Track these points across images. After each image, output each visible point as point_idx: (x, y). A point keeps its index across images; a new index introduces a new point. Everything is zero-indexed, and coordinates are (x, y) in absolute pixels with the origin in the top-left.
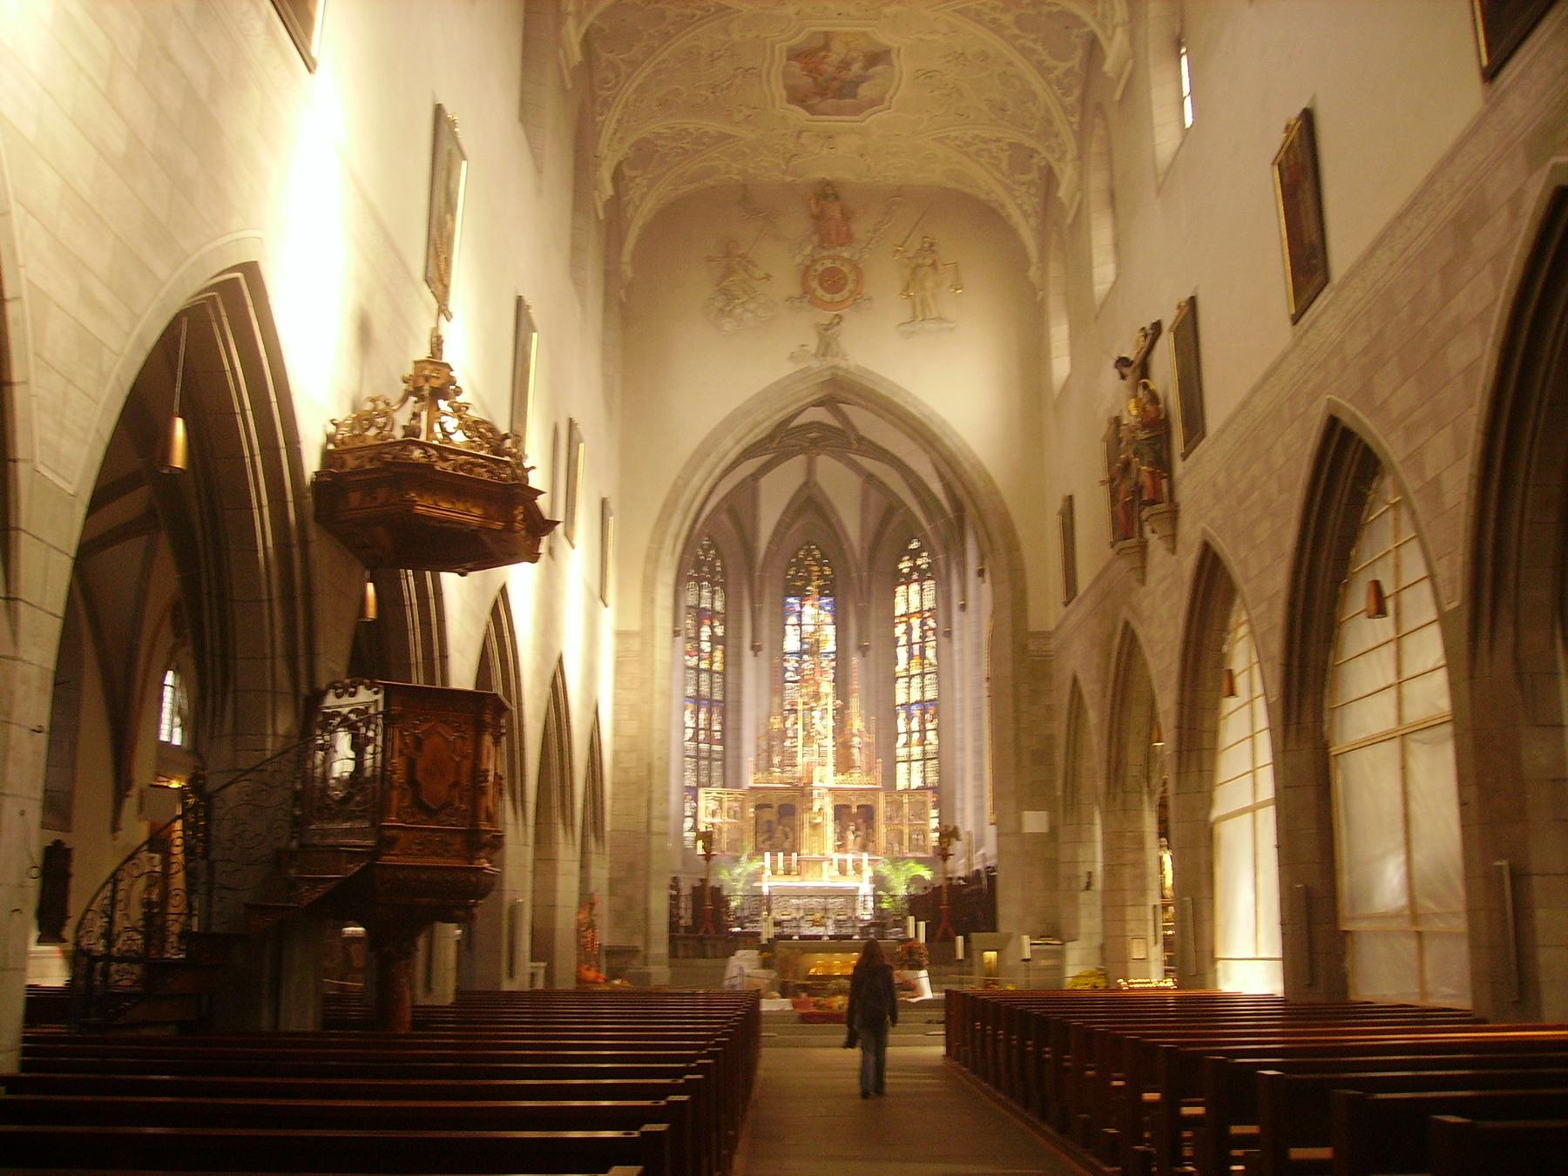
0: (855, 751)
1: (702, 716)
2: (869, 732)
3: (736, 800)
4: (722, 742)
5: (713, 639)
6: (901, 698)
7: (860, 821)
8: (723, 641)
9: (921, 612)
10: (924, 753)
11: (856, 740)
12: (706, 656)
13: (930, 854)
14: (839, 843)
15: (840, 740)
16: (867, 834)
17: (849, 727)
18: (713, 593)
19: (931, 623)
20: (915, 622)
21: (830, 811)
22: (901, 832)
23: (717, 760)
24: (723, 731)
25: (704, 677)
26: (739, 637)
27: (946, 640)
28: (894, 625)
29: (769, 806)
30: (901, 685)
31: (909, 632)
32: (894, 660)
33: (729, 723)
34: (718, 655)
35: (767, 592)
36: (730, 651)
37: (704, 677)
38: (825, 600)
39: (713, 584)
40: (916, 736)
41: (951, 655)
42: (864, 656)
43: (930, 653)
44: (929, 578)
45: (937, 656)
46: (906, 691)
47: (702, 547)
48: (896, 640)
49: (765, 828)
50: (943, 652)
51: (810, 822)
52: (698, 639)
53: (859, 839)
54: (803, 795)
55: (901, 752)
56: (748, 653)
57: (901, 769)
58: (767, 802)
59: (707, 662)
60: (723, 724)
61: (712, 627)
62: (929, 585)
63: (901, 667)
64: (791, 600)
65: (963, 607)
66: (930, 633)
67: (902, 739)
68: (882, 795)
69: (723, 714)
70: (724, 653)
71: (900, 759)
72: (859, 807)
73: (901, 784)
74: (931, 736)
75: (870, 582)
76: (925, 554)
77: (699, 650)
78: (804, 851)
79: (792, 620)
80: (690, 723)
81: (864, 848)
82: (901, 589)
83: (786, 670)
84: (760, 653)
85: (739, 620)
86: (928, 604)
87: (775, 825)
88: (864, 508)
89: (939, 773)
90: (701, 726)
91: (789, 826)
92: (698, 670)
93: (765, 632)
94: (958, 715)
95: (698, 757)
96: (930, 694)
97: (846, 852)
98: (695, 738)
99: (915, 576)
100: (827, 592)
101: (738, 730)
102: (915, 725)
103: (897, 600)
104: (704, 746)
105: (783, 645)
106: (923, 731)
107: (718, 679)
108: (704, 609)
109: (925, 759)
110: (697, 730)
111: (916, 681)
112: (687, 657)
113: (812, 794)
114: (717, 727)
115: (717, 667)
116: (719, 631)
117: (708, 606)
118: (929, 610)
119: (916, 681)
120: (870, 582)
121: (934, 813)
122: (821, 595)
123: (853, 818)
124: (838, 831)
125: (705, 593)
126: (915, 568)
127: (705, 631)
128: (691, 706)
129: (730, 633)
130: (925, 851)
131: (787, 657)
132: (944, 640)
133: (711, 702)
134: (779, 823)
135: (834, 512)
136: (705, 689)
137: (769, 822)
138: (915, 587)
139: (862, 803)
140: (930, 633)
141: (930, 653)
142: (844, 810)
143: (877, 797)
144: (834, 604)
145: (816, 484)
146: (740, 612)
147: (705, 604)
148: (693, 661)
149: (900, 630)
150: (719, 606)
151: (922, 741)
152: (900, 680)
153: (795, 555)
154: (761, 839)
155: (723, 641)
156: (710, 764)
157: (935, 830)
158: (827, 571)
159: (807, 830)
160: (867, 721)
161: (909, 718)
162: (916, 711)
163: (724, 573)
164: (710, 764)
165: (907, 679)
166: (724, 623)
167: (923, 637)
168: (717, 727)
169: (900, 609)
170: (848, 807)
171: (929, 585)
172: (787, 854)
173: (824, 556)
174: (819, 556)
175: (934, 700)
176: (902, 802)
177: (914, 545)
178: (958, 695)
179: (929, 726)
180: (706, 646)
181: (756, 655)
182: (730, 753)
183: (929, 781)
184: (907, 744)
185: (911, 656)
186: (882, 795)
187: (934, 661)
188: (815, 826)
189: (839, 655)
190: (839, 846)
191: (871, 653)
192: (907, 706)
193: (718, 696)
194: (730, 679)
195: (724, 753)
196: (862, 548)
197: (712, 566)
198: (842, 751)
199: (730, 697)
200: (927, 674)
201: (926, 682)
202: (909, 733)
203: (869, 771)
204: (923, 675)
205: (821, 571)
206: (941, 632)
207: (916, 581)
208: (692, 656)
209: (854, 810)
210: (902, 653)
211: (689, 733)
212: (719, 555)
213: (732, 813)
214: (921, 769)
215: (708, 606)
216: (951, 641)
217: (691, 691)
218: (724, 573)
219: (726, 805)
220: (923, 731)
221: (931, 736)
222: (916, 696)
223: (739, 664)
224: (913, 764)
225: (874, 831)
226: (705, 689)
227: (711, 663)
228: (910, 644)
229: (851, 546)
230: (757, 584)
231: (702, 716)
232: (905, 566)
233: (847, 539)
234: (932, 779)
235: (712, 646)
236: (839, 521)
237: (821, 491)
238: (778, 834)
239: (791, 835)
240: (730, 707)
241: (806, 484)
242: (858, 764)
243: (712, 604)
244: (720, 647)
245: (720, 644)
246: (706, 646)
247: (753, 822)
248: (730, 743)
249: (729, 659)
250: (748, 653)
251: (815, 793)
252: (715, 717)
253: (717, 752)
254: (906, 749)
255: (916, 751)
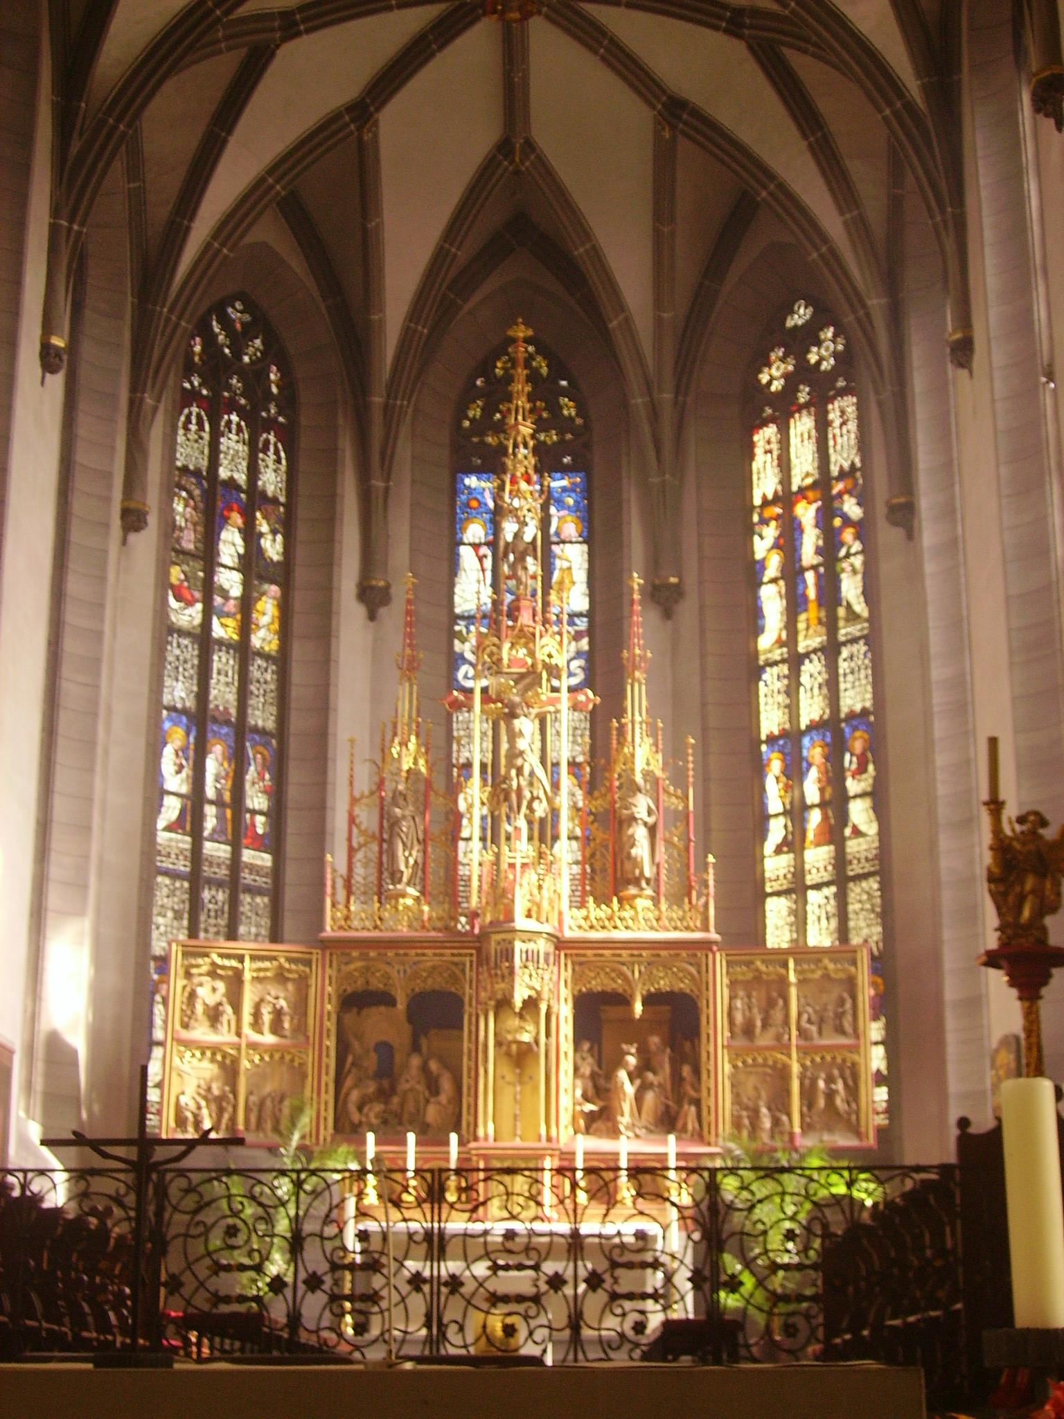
0: (640, 833)
1: (213, 765)
2: (679, 778)
3: (281, 977)
4: (275, 843)
5: (251, 563)
6: (771, 720)
7: (655, 1040)
8: (283, 574)
9: (823, 483)
10: (840, 861)
11: (641, 805)
12: (231, 606)
13: (871, 1141)
14: (589, 1107)
15: (599, 804)
16: (677, 1078)
17: (619, 768)
18: (255, 450)
19: (851, 508)
20: (806, 513)
21: (565, 1012)
22: (783, 1074)
23: (253, 891)
24: (276, 814)
25: (223, 662)
26: (327, 563)
27: (897, 534)
28: (749, 531)
29: (385, 999)
30: (771, 683)
31: (789, 541)
32: (755, 625)
33: (293, 793)
34: (267, 610)
35: (404, 450)
36: (300, 599)
37: (223, 662)
38: (559, 483)
39: (255, 425)
40: (815, 818)
41: (914, 574)
42: (668, 614)
43: (851, 588)
44: (842, 393)
45: (869, 593)
46: (782, 699)
47: (226, 323)
48: (762, 565)
49: (371, 1062)
50: (888, 568)
51: (498, 1044)
52: (208, 556)
53: (650, 1097)
54: (482, 958)
55: (776, 866)
56: (350, 611)
57: (777, 911)
58: (377, 984)
59: (231, 622)
60: (277, 794)
61: (250, 535)
62: (843, 409)
63: (767, 641)
64: (472, 481)
65: (963, 351)
66: (848, 535)
67: (777, 830)
68: (719, 962)
69: (279, 768)
70: (285, 609)
71: (776, 887)
72: (648, 1001)
73: (778, 933)
74: (860, 813)
75: (680, 426)
76: (829, 333)
77: (209, 589)
78: (487, 1128)
79: (475, 531)
80: (175, 781)
81: (667, 1122)
82: (766, 436)
83: (458, 659)
84: (383, 611)
85: (330, 521)
86: (843, 454)
87: (398, 1058)
88: (663, 209)
89: (886, 915)
90: (210, 793)
91: (442, 1060)
92: (204, 640)
93: (399, 553)
94: (940, 728)
95: (196, 879)
96: (855, 697)
97: (614, 1133)
98: (191, 820)
99: (803, 397)
100: (567, 460)
101: (319, 808)
102: (812, 790)
103: (756, 466)
104: (216, 850)
105: (452, 585)
106: (836, 803)
107: (263, 675)
108: (231, 483)
109: (841, 878)
110: (196, 800)
111: (812, 670)
112: (172, 602)
113: (508, 955)
114: (257, 800)
115: (264, 638)
116: (273, 548)
117: (241, 478)
118: (843, 475)
119: (812, 670)
120: (680, 426)
121: (876, 1030)
122: (547, 461)
123: (634, 1031)
124: (586, 1070)
125: (232, 444)
126: (803, 373)
127: (231, 543)
128: (177, 737)
129: (300, 553)
130: (857, 1132)
131: (460, 627)
132: (888, 535)
133: (241, 730)
134: (416, 1047)
135: (586, 235)
136: (223, 693)
137: (385, 1049)
138: (803, 425)
139: (664, 985)
140: (848, 535)
141: (851, 588)
142: (611, 1012)
143: (703, 969)
144: (588, 491)
145: (530, 146)
146: (331, 500)
147: (232, 469)
148: (188, 616)
149: (764, 544)
150: (271, 480)
151: (835, 831)
152: (770, 675)
153: (485, 368)
154: (355, 1096)
155: (283, 574)
156: (234, 902)
157: (879, 1079)
158: (569, 408)
159: (491, 1067)
160: (673, 753)
161: (794, 771)
162: (814, 752)
163: (288, 401)
164: (234, 902)
165: (784, 669)
166: (287, 527)
167: (830, 548)
168: (257, 800)
169: (765, 483)
170: (623, 1001)
171: (843, 409)
172: (432, 1137)
173: (559, 370)
174: (544, 371)
175: (865, 712)
176: (783, 982)
177: (801, 315)
178: (938, 672)
179: (853, 786)
180: (230, 581)
181: (372, 616)
182: (291, 873)
183: (855, 940)
184: (793, 844)
185: (795, 604)
186: (719, 962)
187: (860, 607)
188: (521, 1057)
189: (599, 618)
190: (591, 1118)
191: (687, 609)
192: (790, 739)
193: (262, 716)
194: (298, 675)
195: (277, 871)
196: (658, 322)
197: (255, 377)
198: (600, 835)
199: (297, 723)
200: (844, 644)
201: (843, 666)
202: (797, 812)
203: (683, 892)
204: (831, 650)
205: (555, 409)
206: (881, 509)
207: (807, 406)
208: (190, 603)
209: (638, 1008)
210: (772, 600)
211: (171, 809)
212: (275, 352)
213: (267, 1018)
214: (832, 907)
215: (241, 478)
216: (911, 534)
217: (179, 692)
218: (288, 401)
219: (249, 996)
220: (836, 803)
221: (860, 813)
222: (812, 708)
223: (324, 636)
224: (811, 894)
225: (697, 1071)
226: (223, 693)
227: (246, 628)
228: (792, 573)
229: (628, 323)
230: (377, 432)
231: (213, 765)
232: (774, 375)
233: (621, 307)
234: (866, 930)
235: (246, 584)
236: (596, 254)
237: (542, 162)
238: (411, 1080)
239: (446, 1085)
240: (294, 747)
241: (504, 147)
242: (648, 872)
243: (253, 471)
244: (274, 590)
245: (272, 582)
246: (230, 581)
247: (331, 1043)
248: (292, 845)
249: (298, 624)
250: (350, 611)
251: (519, 946)
252: (251, 773)
253: (253, 868)
254: (786, 860)
255: (818, 858)
